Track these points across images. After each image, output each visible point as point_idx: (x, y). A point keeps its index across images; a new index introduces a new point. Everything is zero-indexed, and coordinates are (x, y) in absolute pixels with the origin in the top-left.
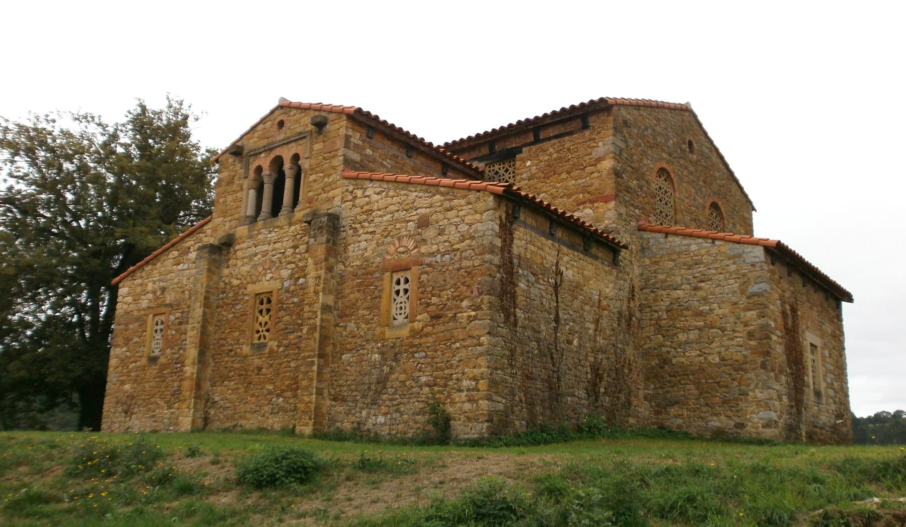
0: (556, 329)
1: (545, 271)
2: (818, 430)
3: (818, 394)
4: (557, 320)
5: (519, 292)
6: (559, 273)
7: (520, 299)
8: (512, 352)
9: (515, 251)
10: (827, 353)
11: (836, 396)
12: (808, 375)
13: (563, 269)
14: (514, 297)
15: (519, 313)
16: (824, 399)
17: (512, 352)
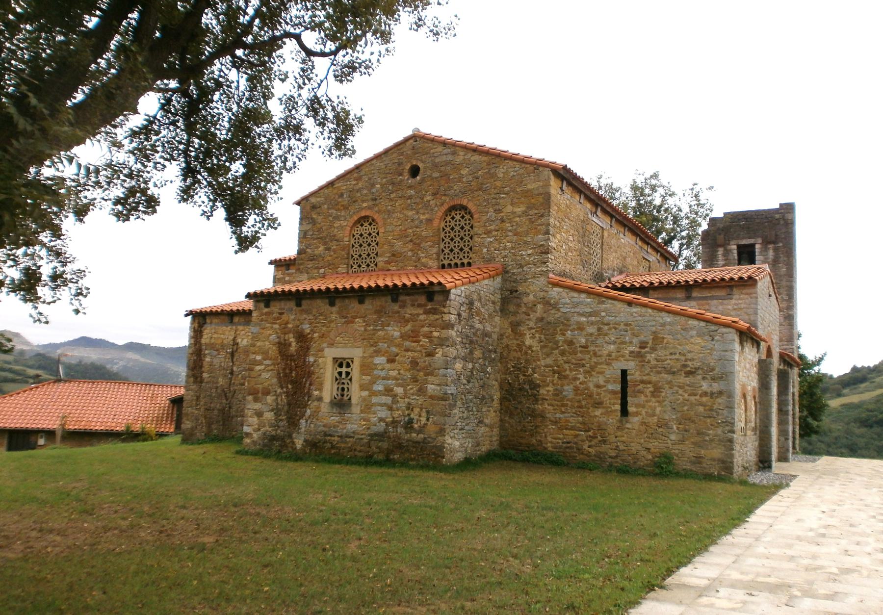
0: (231, 379)
1: (223, 346)
2: (336, 438)
3: (341, 404)
4: (232, 373)
5: (205, 363)
6: (235, 343)
7: (206, 367)
8: (198, 398)
9: (203, 341)
10: (380, 360)
11: (395, 402)
12: (320, 389)
13: (239, 340)
14: (201, 367)
15: (205, 375)
16: (356, 409)
17: (198, 398)
